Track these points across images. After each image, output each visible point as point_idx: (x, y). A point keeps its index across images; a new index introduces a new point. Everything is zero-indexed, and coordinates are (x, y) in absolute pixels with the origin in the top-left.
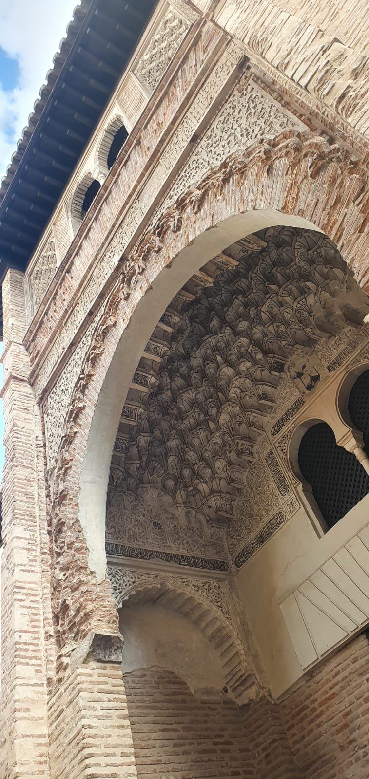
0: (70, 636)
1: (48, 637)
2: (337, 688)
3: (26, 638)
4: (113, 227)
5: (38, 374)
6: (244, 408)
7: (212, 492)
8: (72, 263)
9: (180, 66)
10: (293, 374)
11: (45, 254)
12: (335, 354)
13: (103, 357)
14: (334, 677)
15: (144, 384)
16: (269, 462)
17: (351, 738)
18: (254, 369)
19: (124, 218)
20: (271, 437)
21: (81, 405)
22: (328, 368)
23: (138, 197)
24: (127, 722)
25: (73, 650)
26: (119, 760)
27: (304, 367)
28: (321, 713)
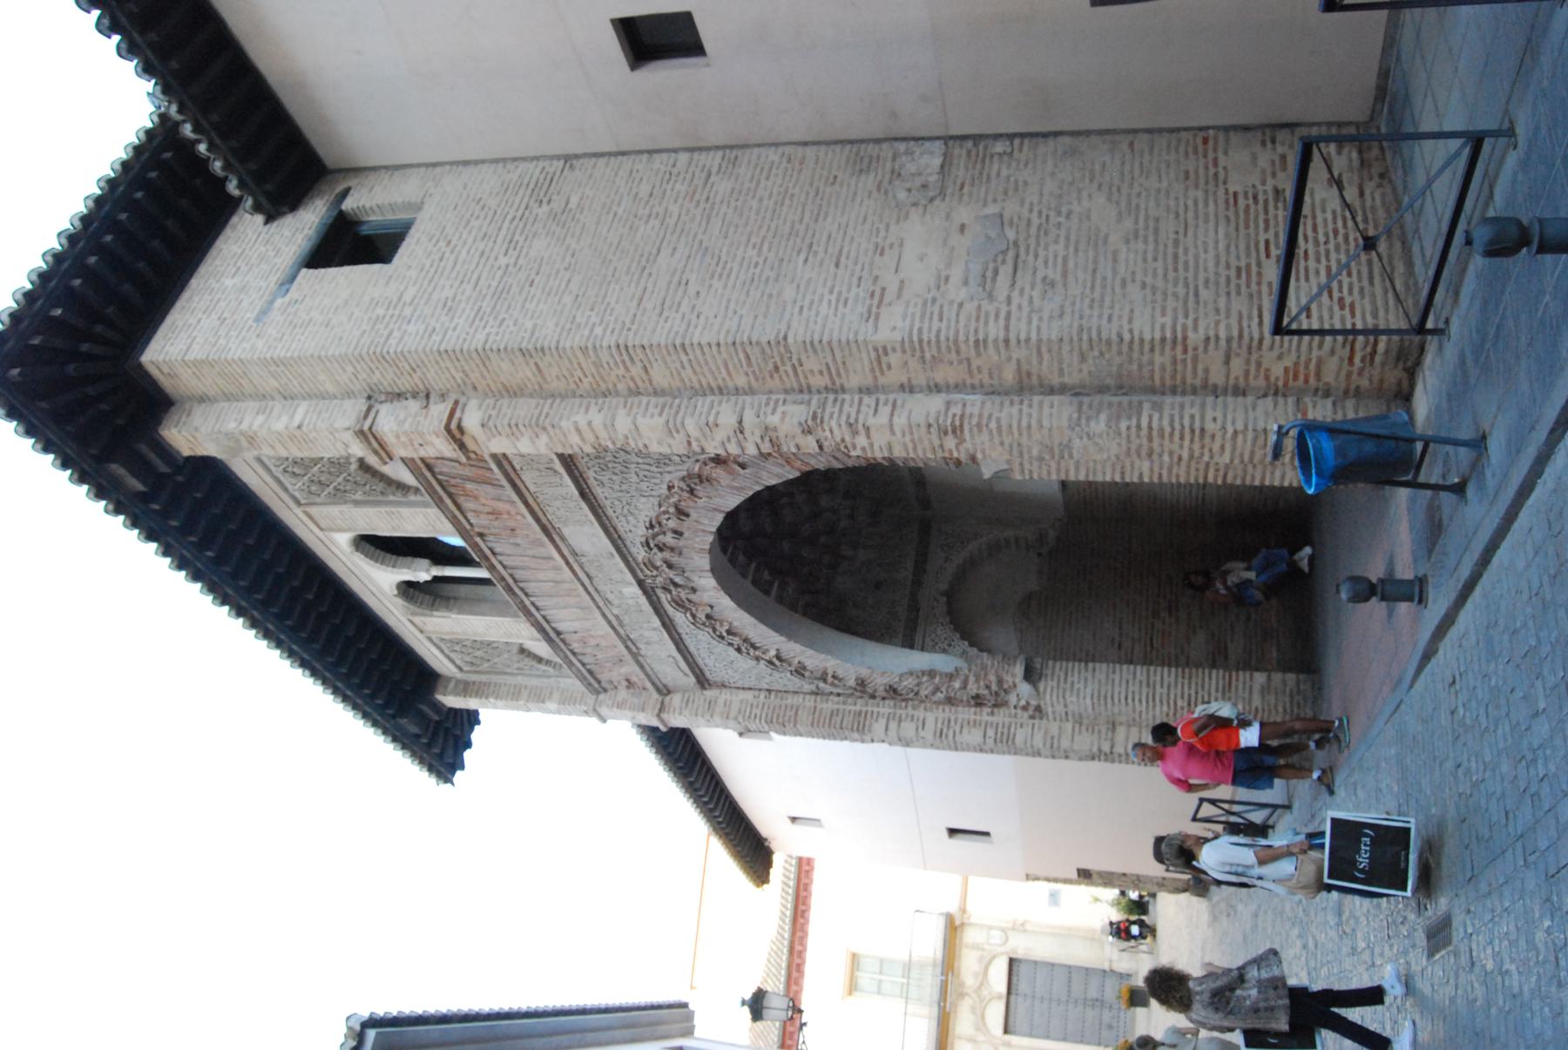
1: (992, 713)
3: (990, 733)
4: (583, 585)
7: (851, 517)
13: (735, 624)
15: (771, 584)
21: (773, 653)
23: (575, 554)
24: (1091, 665)
26: (1117, 677)
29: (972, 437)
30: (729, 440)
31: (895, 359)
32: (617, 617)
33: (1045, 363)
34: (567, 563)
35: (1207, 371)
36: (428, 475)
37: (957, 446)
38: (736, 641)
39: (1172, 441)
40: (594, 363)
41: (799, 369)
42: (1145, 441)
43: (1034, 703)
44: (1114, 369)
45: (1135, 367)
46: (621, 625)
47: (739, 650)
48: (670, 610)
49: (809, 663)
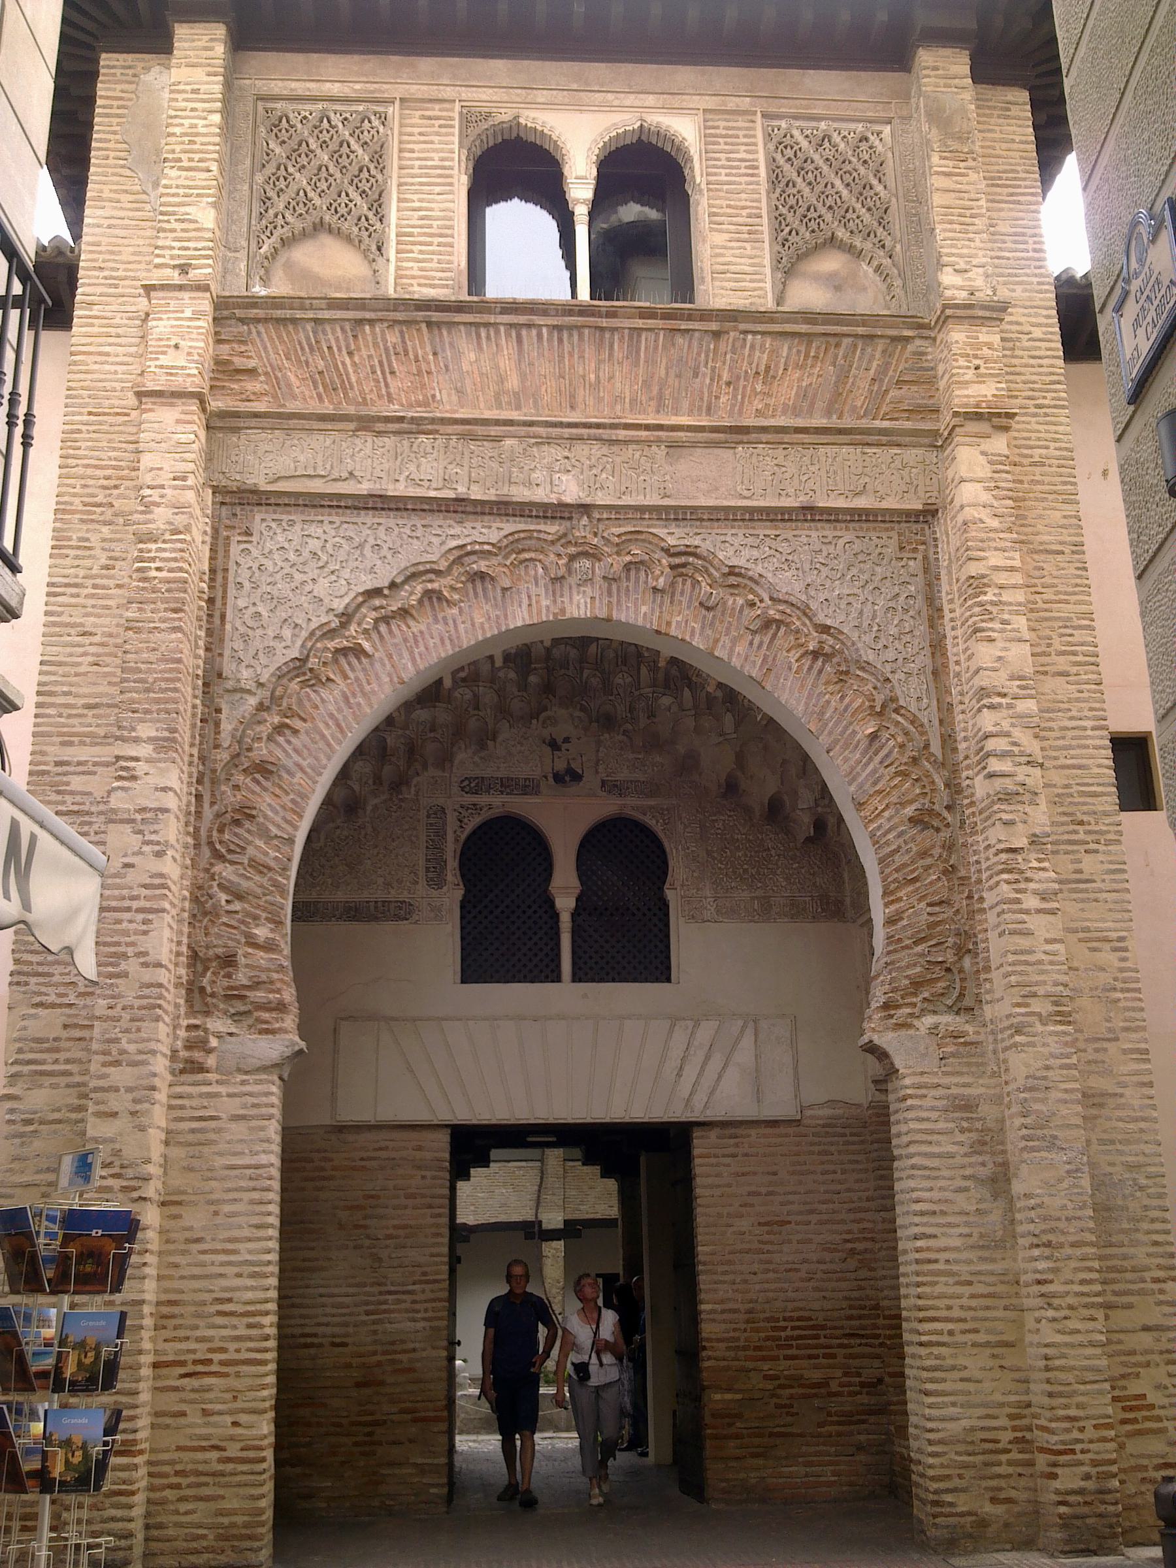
0: (222, 1006)
2: (374, 1163)
4: (598, 426)
5: (240, 428)
6: (459, 732)
8: (451, 325)
9: (856, 336)
10: (546, 733)
11: (332, 115)
12: (623, 775)
14: (375, 1150)
16: (432, 821)
17: (362, 1222)
18: (515, 690)
19: (626, 442)
20: (455, 789)
21: (366, 645)
22: (603, 783)
23: (672, 446)
25: (231, 1034)
27: (567, 740)
28: (331, 1178)
29: (1057, 1033)
30: (1015, 744)
31: (1108, 957)
32: (497, 439)
33: (1121, 1124)
34: (660, 427)
35: (1130, 1306)
36: (860, 330)
37: (1039, 1015)
38: (411, 594)
39: (1076, 1270)
40: (1069, 619)
41: (1082, 848)
42: (1072, 1239)
43: (211, 1061)
44: (1120, 1203)
45: (1125, 1226)
46: (462, 436)
47: (376, 592)
48: (510, 526)
49: (330, 698)
